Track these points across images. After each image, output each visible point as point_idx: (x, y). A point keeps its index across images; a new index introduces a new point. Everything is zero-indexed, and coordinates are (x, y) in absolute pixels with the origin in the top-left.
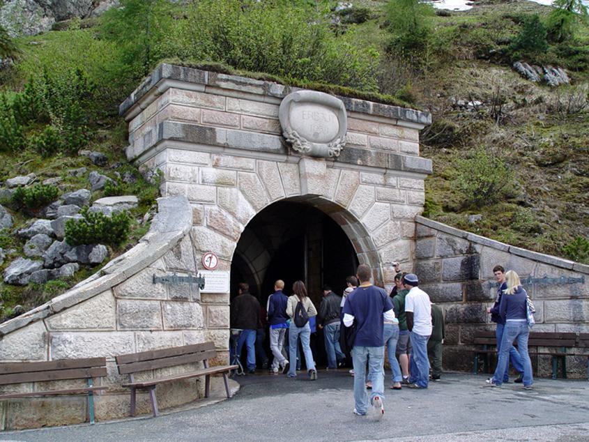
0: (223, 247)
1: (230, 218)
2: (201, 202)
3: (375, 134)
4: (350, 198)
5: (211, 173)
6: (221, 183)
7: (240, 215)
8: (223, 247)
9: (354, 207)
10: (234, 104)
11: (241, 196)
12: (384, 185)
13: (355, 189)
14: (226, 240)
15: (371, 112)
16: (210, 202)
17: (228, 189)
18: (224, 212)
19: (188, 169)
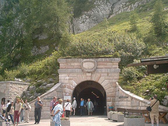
0: (70, 91)
1: (72, 86)
2: (66, 83)
3: (106, 65)
4: (99, 80)
5: (67, 78)
6: (69, 79)
7: (73, 85)
8: (70, 91)
9: (100, 82)
10: (73, 64)
11: (74, 82)
12: (108, 76)
13: (100, 77)
14: (71, 90)
15: (103, 61)
16: (68, 83)
17: (71, 81)
18: (70, 85)
19: (63, 78)
